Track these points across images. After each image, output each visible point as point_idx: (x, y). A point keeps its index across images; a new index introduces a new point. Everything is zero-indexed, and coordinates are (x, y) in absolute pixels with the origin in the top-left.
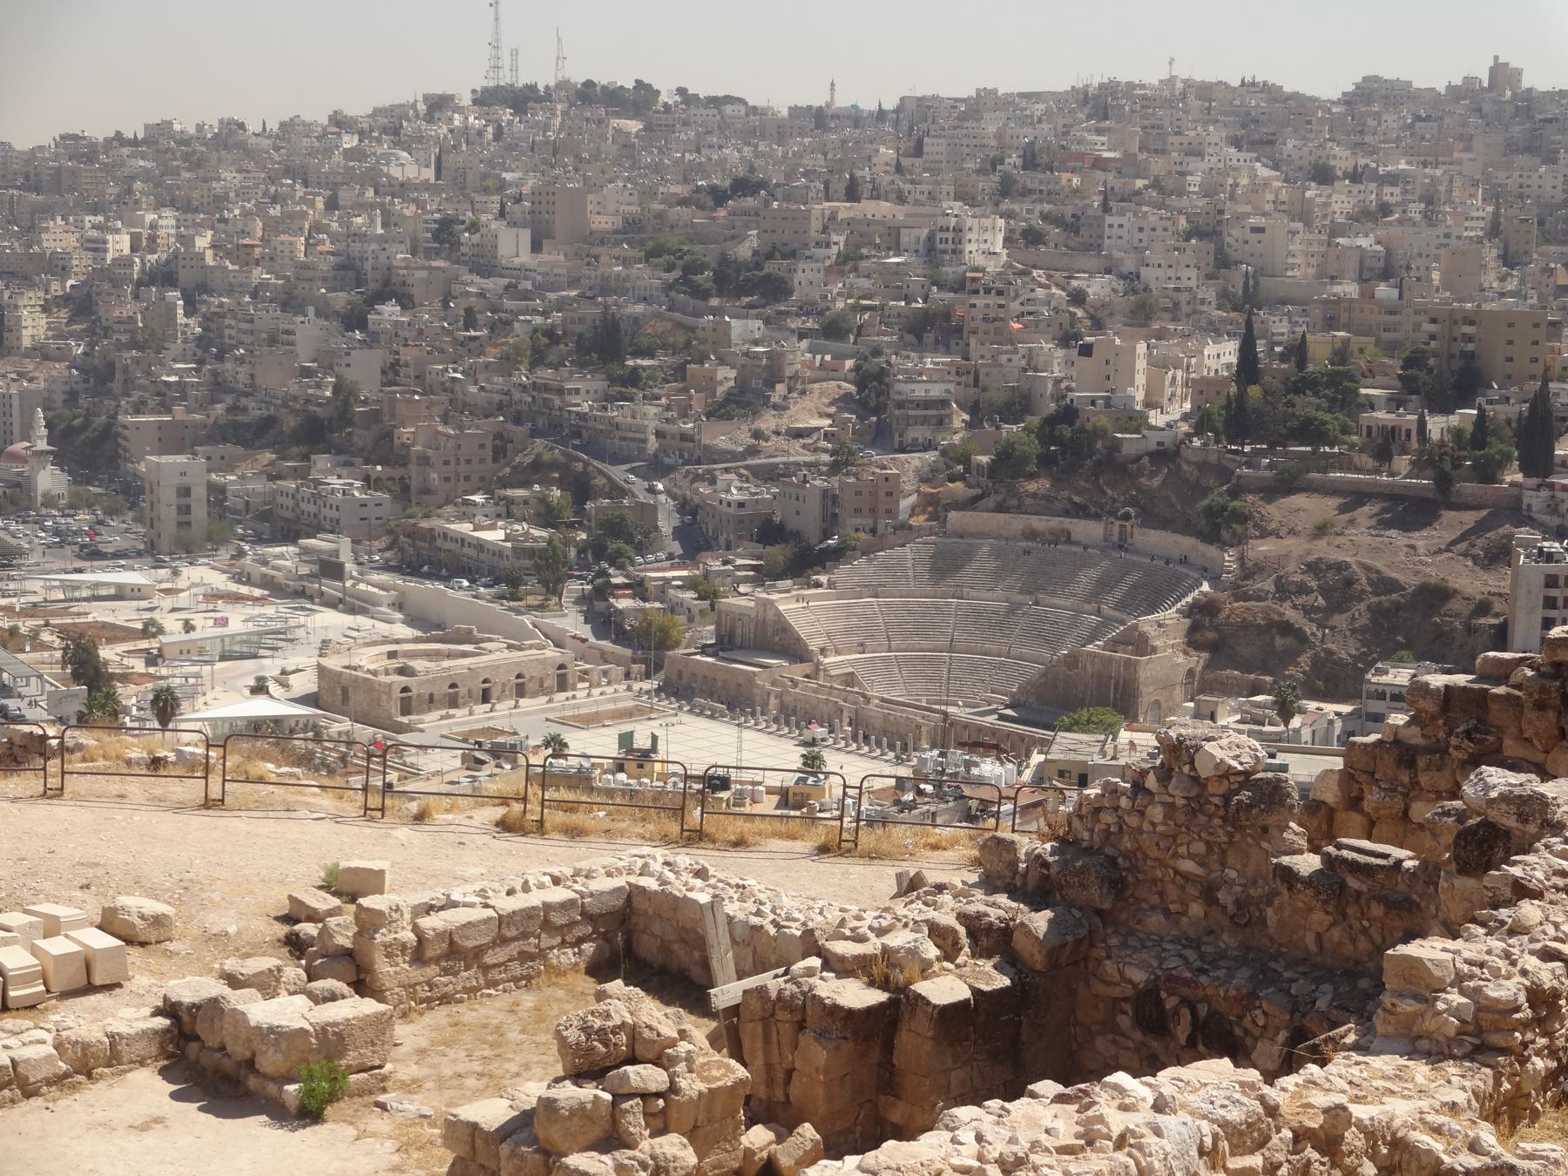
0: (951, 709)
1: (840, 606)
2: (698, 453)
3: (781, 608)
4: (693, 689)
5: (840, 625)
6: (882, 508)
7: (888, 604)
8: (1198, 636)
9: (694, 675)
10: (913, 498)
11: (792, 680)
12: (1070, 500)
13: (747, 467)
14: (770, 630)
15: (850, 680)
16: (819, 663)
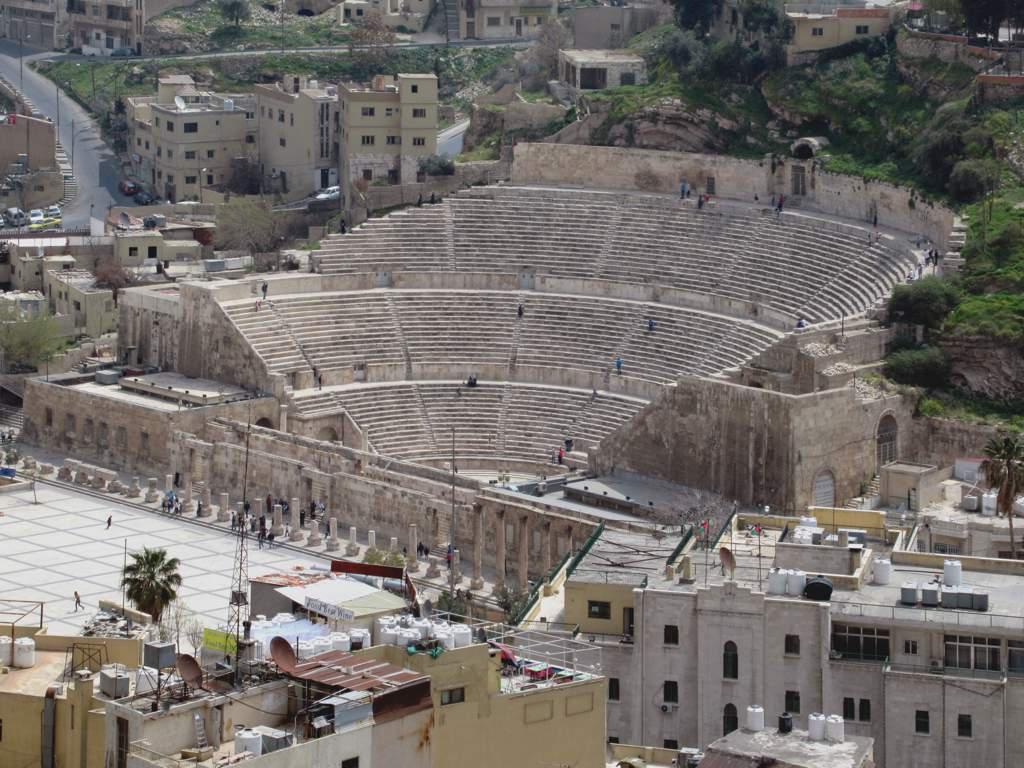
0: (484, 477)
1: (323, 302)
2: (136, 38)
3: (222, 305)
4: (69, 441)
5: (326, 333)
6: (407, 140)
7: (409, 298)
8: (905, 356)
9: (71, 416)
10: (464, 125)
11: (235, 428)
13: (216, 65)
14: (205, 341)
15: (336, 429)
16: (283, 398)
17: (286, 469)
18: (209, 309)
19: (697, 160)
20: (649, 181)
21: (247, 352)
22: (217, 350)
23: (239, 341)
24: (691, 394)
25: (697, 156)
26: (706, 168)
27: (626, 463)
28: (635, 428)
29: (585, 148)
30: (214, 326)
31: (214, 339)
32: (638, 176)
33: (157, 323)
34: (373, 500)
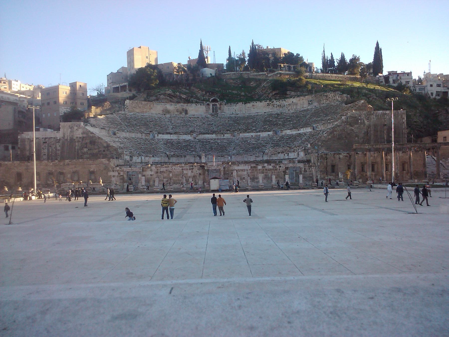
12: (181, 98)
14: (77, 145)
17: (192, 169)
18: (80, 131)
19: (182, 105)
20: (168, 112)
21: (105, 145)
22: (86, 147)
23: (99, 141)
24: (356, 117)
25: (182, 104)
26: (184, 107)
27: (323, 149)
28: (328, 135)
29: (146, 102)
30: (84, 137)
31: (84, 142)
32: (163, 111)
33: (46, 142)
34: (249, 171)
